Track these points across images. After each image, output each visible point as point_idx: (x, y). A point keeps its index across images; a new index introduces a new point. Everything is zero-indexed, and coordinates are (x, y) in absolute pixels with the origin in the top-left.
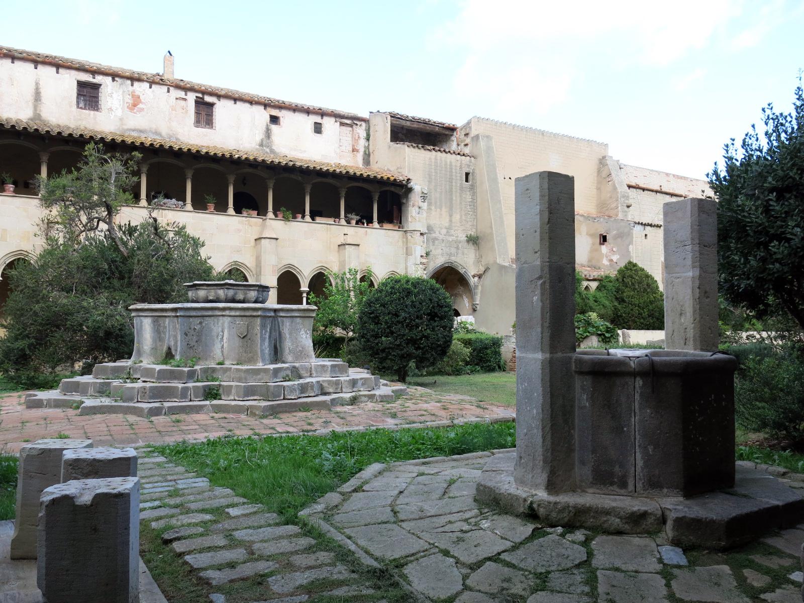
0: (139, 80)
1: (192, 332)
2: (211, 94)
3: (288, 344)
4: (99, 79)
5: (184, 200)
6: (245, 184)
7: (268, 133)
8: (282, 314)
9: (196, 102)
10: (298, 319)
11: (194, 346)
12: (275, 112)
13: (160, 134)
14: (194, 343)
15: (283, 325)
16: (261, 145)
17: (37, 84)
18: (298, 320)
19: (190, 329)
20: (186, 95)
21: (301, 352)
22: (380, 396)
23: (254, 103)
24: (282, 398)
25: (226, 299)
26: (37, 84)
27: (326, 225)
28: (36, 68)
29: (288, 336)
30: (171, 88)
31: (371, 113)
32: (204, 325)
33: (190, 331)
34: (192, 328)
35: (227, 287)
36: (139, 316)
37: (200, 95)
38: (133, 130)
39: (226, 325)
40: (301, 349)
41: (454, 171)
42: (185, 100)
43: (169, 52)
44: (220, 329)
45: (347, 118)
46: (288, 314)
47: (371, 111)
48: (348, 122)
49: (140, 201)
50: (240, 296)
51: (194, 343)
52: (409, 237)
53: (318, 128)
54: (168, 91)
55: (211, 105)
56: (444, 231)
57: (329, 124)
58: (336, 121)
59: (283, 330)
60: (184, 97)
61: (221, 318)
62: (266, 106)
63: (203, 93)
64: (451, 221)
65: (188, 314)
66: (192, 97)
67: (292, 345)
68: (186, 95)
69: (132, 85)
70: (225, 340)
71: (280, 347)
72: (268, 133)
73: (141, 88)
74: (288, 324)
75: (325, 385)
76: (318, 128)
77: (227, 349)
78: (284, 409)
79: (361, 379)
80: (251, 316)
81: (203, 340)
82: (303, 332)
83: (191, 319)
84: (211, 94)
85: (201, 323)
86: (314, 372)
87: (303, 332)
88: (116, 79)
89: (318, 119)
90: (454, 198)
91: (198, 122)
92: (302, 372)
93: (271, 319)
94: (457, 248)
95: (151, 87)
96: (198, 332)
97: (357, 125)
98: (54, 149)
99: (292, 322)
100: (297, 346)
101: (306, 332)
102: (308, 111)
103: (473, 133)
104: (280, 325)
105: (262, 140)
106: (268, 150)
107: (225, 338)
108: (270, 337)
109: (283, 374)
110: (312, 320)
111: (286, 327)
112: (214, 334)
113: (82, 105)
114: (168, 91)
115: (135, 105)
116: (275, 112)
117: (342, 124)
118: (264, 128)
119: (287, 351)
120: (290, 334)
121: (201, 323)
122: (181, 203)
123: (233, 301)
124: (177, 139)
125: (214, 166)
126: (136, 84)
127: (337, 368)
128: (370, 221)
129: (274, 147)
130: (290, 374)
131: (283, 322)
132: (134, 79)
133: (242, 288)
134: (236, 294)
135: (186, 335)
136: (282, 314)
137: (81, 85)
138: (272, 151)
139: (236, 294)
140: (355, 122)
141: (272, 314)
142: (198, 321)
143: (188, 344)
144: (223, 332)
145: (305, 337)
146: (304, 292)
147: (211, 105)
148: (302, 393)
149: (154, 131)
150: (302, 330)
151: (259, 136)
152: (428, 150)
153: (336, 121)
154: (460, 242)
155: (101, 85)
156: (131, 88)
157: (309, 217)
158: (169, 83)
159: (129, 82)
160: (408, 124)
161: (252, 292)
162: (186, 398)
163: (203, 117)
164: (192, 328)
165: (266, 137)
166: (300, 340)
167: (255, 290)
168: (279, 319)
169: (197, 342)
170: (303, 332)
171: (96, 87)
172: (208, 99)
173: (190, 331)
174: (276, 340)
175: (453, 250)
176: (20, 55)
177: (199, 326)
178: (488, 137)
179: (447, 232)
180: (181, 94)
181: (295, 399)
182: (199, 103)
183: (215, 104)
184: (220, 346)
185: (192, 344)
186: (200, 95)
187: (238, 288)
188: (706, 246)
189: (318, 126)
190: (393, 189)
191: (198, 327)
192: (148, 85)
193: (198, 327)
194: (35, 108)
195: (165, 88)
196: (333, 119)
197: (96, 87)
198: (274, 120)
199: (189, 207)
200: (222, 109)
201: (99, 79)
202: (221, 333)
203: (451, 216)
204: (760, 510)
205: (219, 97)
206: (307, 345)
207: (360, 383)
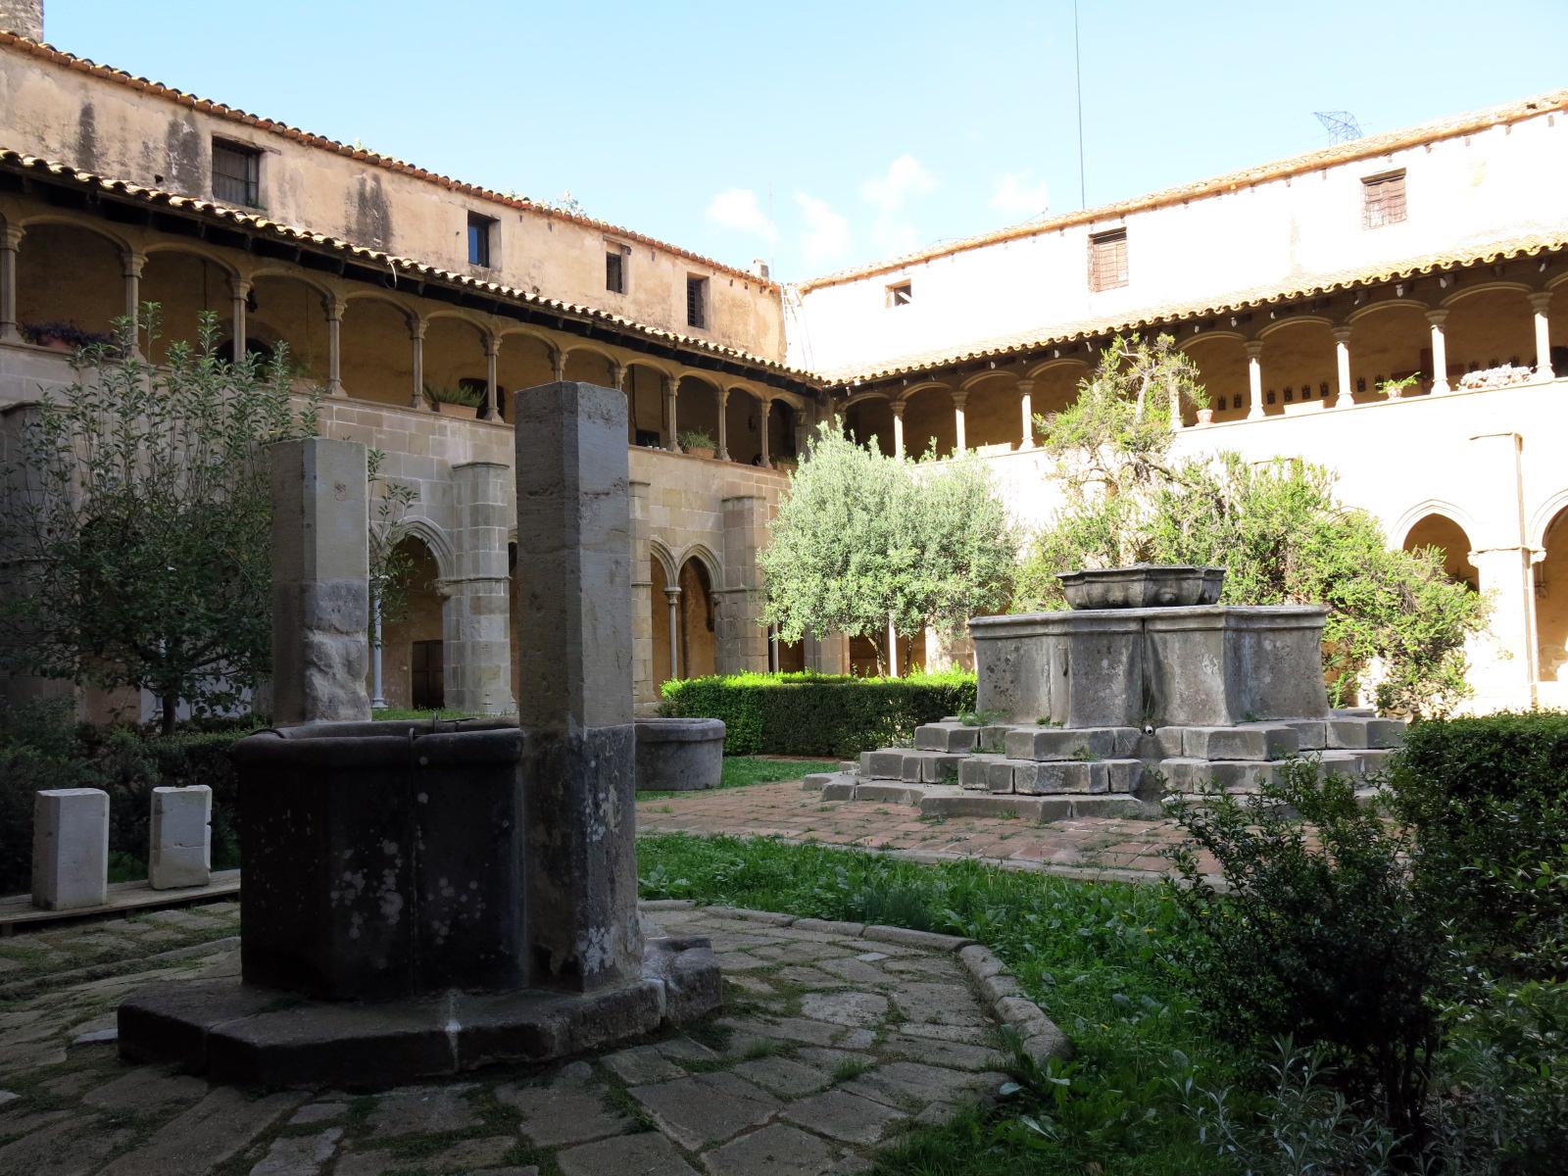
1: (1003, 665)
3: (1178, 687)
5: (1533, 363)
8: (1160, 626)
10: (1197, 635)
14: (1008, 685)
15: (1165, 648)
18: (1198, 637)
19: (999, 660)
21: (1204, 703)
24: (1010, 790)
25: (1091, 602)
29: (1177, 670)
32: (1022, 652)
34: (1003, 659)
35: (1087, 579)
40: (1203, 697)
46: (1174, 624)
49: (1337, 397)
50: (1117, 594)
51: (1008, 685)
54: (1551, 123)
59: (1166, 657)
61: (1044, 639)
65: (990, 634)
67: (1188, 688)
71: (1162, 692)
74: (1177, 645)
78: (974, 810)
79: (1252, 767)
80: (1091, 634)
81: (1023, 679)
82: (1206, 662)
83: (1000, 644)
85: (1017, 649)
87: (1206, 662)
93: (1131, 637)
98: (1037, 371)
99: (1185, 641)
100: (1197, 692)
101: (1212, 662)
104: (1160, 650)
108: (1130, 673)
109: (1074, 746)
110: (1221, 635)
111: (1173, 653)
112: (1038, 668)
113: (1376, 218)
114: (1551, 123)
119: (1176, 701)
120: (1183, 666)
121: (1017, 649)
122: (1525, 370)
123: (1107, 604)
125: (869, 395)
127: (1237, 741)
130: (1087, 746)
131: (1165, 643)
133: (1119, 578)
134: (1107, 591)
135: (992, 671)
136: (1160, 626)
139: (1107, 591)
141: (1133, 627)
142: (1011, 645)
144: (1048, 664)
145: (1210, 671)
148: (1066, 785)
150: (1206, 656)
155: (1404, 169)
158: (1549, 106)
161: (1136, 584)
162: (914, 776)
164: (1003, 659)
166: (1202, 677)
167: (1140, 580)
168: (1156, 636)
169: (1012, 682)
170: (1207, 663)
174: (1145, 679)
177: (1014, 655)
181: (1101, 794)
185: (1005, 685)
187: (1110, 579)
188: (536, 493)
191: (1012, 657)
195: (1543, 119)
204: (169, 1017)
206: (1215, 689)
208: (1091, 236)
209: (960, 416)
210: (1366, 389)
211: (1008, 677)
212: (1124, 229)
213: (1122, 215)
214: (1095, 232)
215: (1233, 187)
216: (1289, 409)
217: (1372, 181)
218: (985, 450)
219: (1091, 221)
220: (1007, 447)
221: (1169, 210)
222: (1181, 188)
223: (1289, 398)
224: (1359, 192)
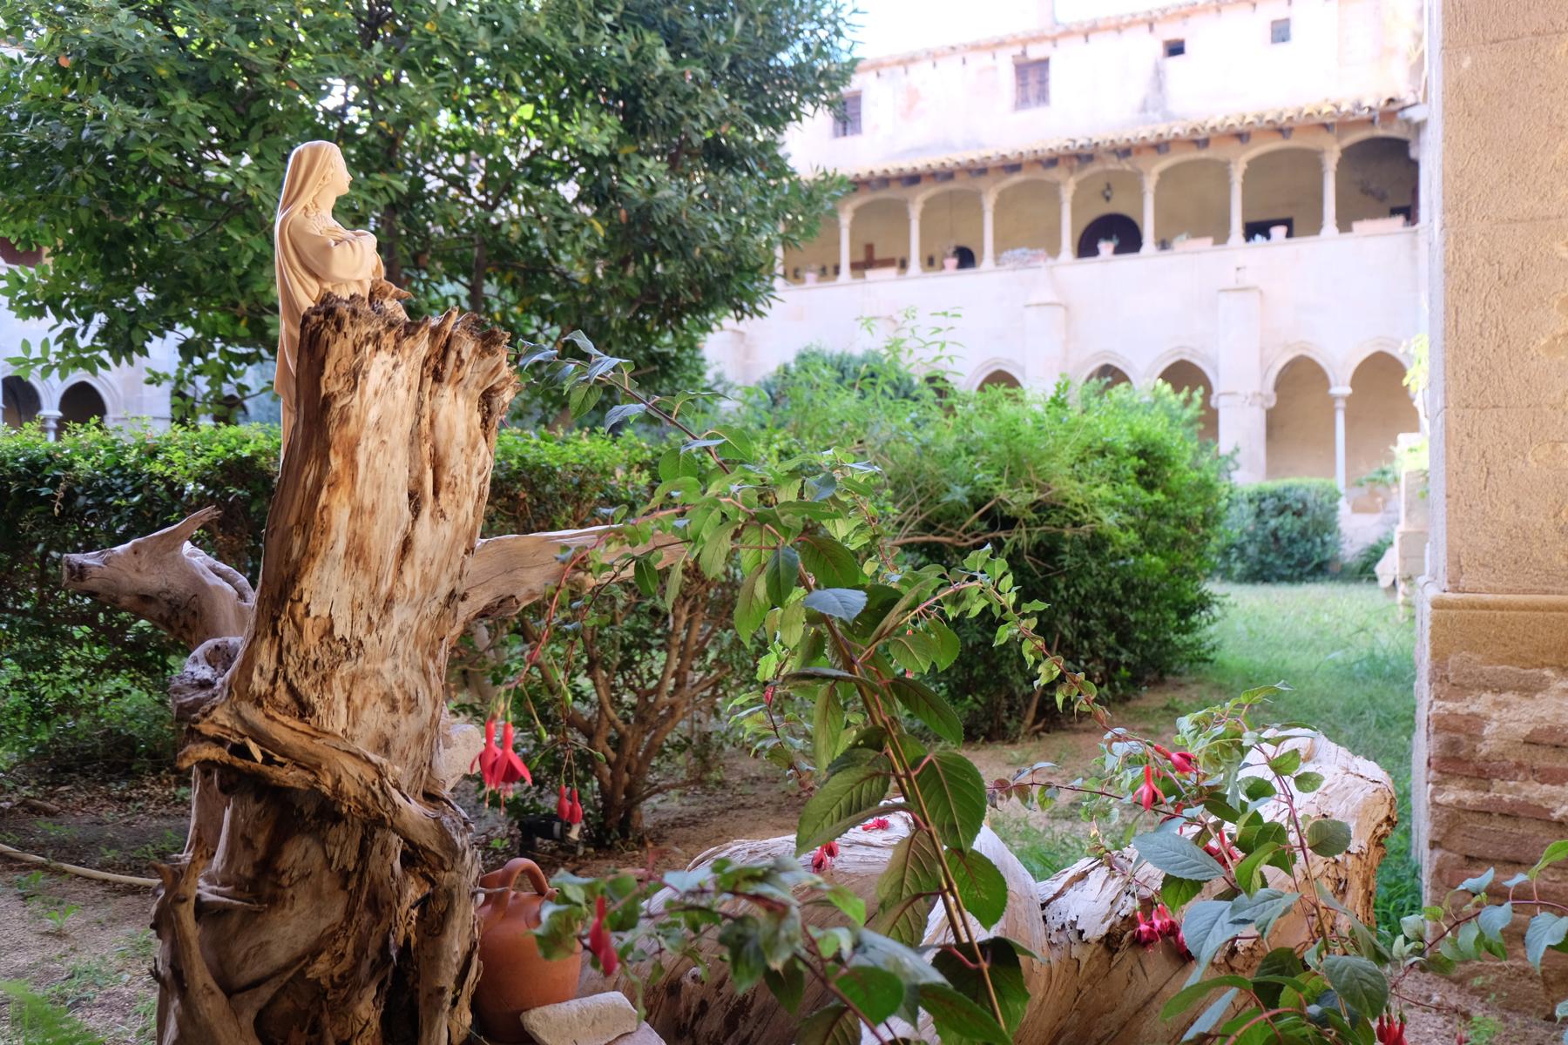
0: (913, 60)
2: (1038, 39)
6: (1108, 199)
7: (1158, 79)
12: (1172, 33)
55: (1043, 63)
63: (1024, 43)
72: (1158, 79)
73: (921, 73)
88: (882, 71)
91: (1022, 102)
105: (1145, 101)
115: (910, 107)
126: (913, 69)
128: (1315, 227)
132: (907, 62)
138: (1167, 117)
147: (1043, 63)
151: (1138, 89)
159: (901, 69)
172: (1035, 53)
180: (986, 59)
195: (957, 60)
200: (1065, 65)
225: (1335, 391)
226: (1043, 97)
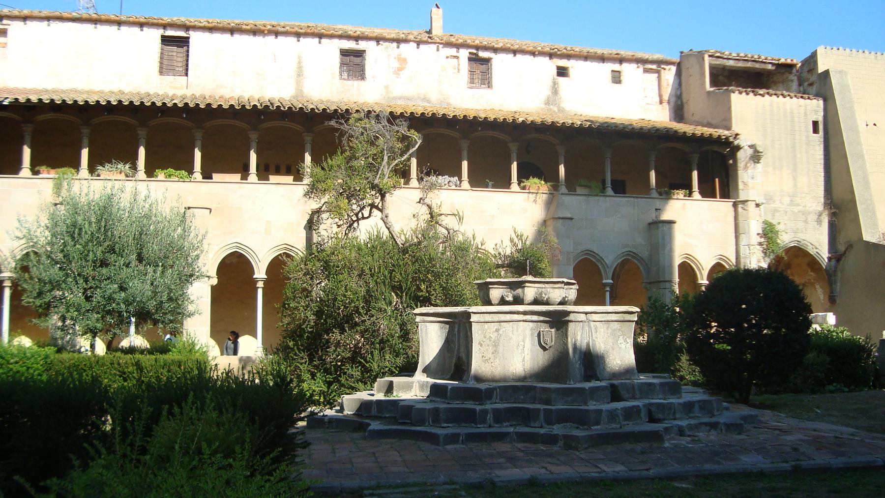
0: (406, 41)
1: (488, 342)
2: (486, 48)
4: (362, 45)
7: (555, 90)
9: (470, 59)
11: (490, 358)
13: (429, 101)
15: (596, 332)
16: (547, 103)
17: (300, 58)
19: (485, 337)
20: (458, 52)
22: (725, 424)
23: (537, 53)
26: (300, 58)
27: (632, 199)
28: (299, 41)
30: (441, 46)
31: (682, 53)
32: (501, 332)
33: (485, 340)
34: (487, 337)
36: (424, 322)
37: (474, 51)
38: (400, 98)
39: (528, 333)
41: (796, 119)
42: (457, 57)
43: (436, 5)
44: (521, 338)
45: (652, 62)
47: (682, 50)
48: (654, 67)
52: (740, 210)
53: (617, 78)
54: (438, 50)
55: (487, 61)
56: (787, 200)
57: (629, 70)
58: (638, 67)
59: (597, 338)
60: (456, 54)
62: (551, 56)
63: (478, 48)
64: (795, 185)
66: (464, 54)
68: (458, 52)
69: (398, 47)
70: (526, 353)
72: (555, 90)
74: (602, 330)
75: (653, 409)
76: (617, 78)
77: (529, 363)
79: (699, 401)
83: (486, 325)
84: (486, 48)
85: (497, 330)
86: (637, 393)
89: (616, 67)
90: (798, 156)
92: (624, 394)
94: (806, 222)
95: (418, 48)
96: (494, 342)
97: (665, 69)
101: (625, 340)
102: (602, 59)
103: (821, 69)
105: (548, 98)
106: (556, 109)
107: (526, 349)
113: (345, 75)
114: (438, 50)
116: (563, 63)
117: (646, 71)
118: (550, 83)
124: (449, 104)
126: (403, 45)
129: (562, 105)
135: (481, 345)
137: (345, 53)
138: (561, 110)
140: (662, 66)
142: (495, 326)
143: (483, 356)
144: (523, 341)
146: (606, 285)
147: (487, 61)
149: (422, 97)
152: (760, 95)
153: (638, 67)
154: (809, 214)
156: (397, 51)
157: (610, 189)
158: (438, 40)
159: (395, 44)
160: (731, 63)
161: (557, 290)
163: (478, 76)
164: (487, 337)
165: (552, 93)
169: (493, 353)
170: (623, 341)
171: (360, 54)
172: (483, 54)
173: (485, 340)
175: (800, 225)
176: (283, 29)
177: (496, 334)
178: (840, 72)
179: (791, 201)
180: (453, 51)
182: (474, 59)
183: (491, 59)
184: (520, 359)
185: (489, 355)
186: (474, 51)
189: (617, 74)
190: (716, 148)
192: (413, 45)
193: (494, 336)
194: (299, 83)
195: (434, 47)
196: (634, 66)
197: (360, 54)
198: (562, 72)
199: (466, 184)
201: (362, 45)
202: (522, 343)
203: (795, 179)
205: (495, 50)
207: (697, 406)
208: (163, 37)
209: (695, 174)
210: (264, 172)
211: (491, 349)
212: (188, 38)
213: (187, 28)
214: (166, 34)
215: (266, 32)
216: (273, 178)
217: (345, 53)
218: (105, 171)
219: (165, 26)
220: (237, 177)
221: (217, 36)
222: (233, 22)
223: (278, 172)
224: (337, 57)
225: (700, 281)
226: (486, 80)
